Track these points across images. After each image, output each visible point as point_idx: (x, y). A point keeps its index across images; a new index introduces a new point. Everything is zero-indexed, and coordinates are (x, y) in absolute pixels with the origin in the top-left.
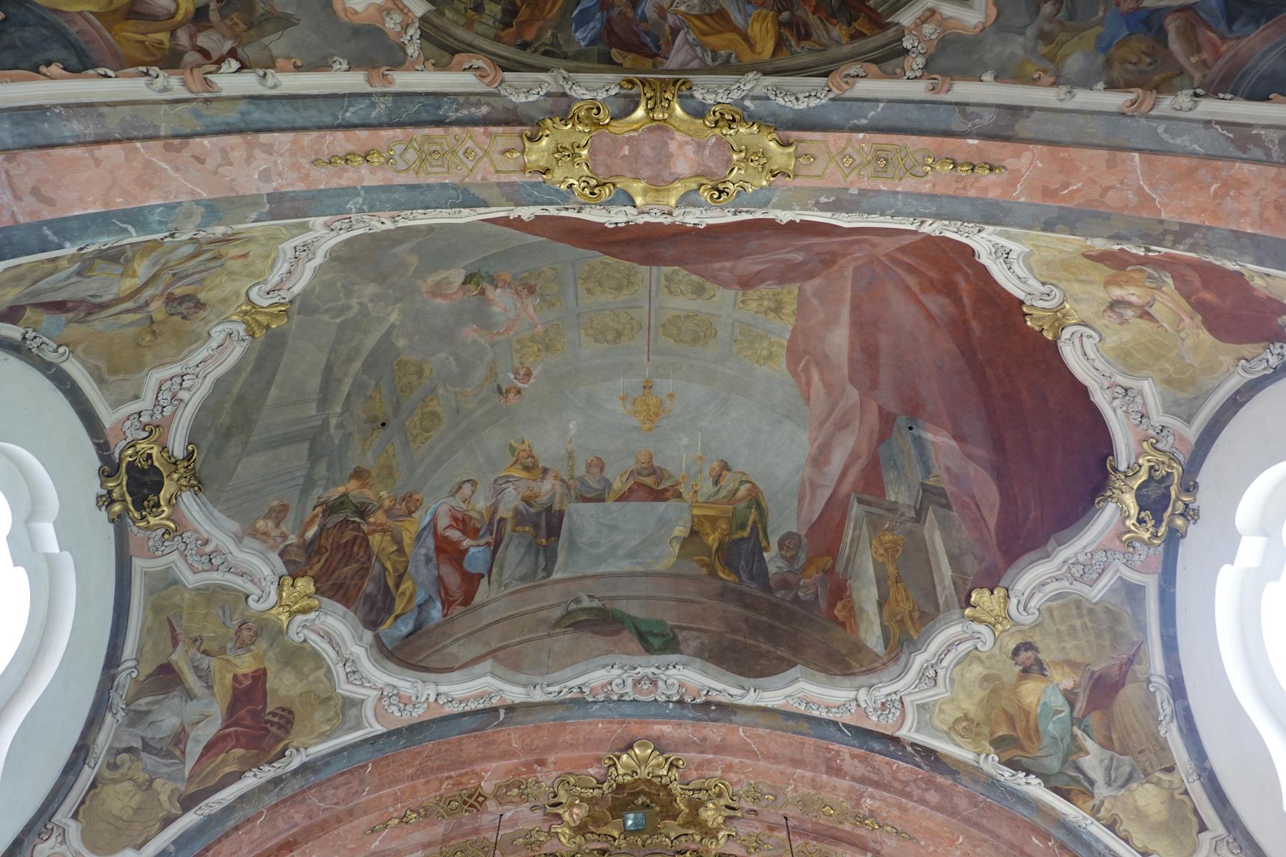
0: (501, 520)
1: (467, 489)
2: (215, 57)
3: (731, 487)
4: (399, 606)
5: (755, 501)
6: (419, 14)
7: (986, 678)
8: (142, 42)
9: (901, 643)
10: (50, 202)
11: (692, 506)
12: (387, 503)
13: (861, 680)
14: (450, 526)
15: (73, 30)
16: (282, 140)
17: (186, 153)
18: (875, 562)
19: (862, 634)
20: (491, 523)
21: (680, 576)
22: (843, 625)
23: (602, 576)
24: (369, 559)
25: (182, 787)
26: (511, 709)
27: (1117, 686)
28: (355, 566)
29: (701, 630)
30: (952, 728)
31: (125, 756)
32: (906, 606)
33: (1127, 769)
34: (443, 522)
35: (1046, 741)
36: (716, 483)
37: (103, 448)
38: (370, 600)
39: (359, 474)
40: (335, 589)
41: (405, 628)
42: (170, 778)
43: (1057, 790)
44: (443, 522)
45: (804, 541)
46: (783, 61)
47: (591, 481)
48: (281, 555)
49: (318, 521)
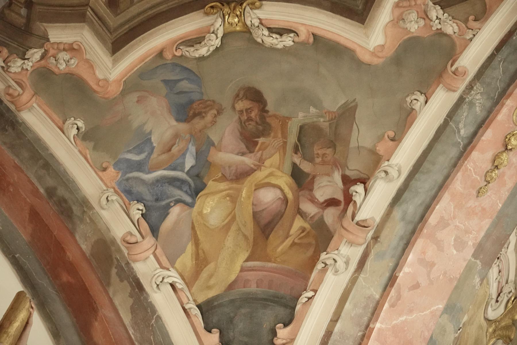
2: (340, 197)
8: (294, 244)
15: (253, 288)
16: (444, 206)
17: (406, 294)
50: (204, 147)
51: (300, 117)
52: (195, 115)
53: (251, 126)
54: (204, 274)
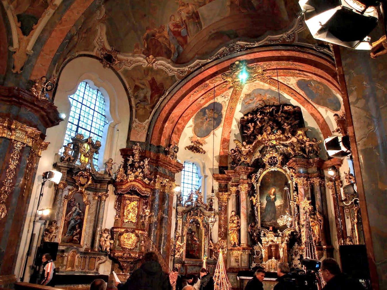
0: (185, 21)
1: (173, 18)
4: (173, 51)
10: (53, 51)
12: (157, 31)
14: (174, 28)
20: (182, 22)
23: (214, 23)
24: (161, 44)
25: (150, 105)
28: (159, 48)
31: (138, 104)
34: (172, 28)
37: (97, 58)
38: (166, 53)
39: (148, 28)
40: (157, 55)
41: (176, 55)
42: (148, 105)
44: (172, 28)
48: (143, 53)
49: (146, 42)
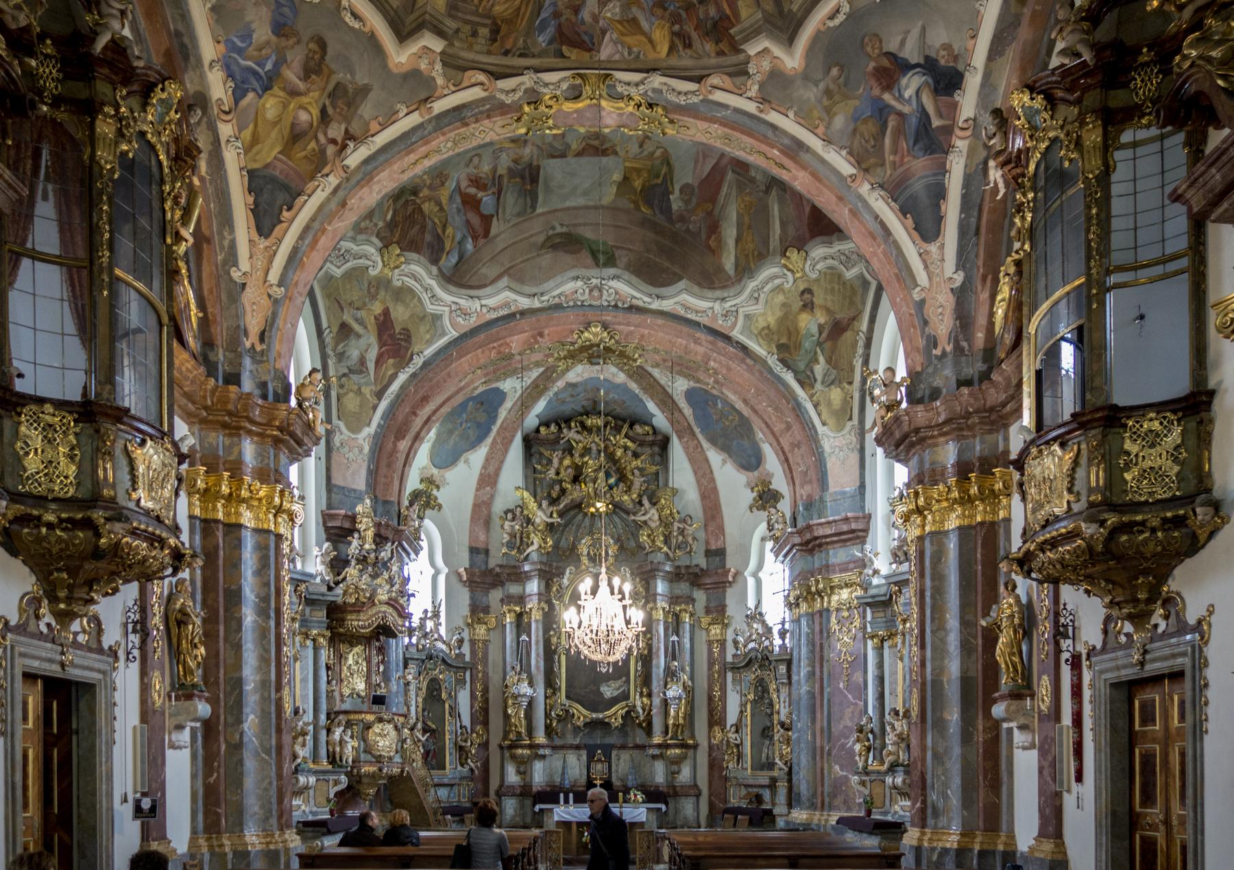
3: (651, 149)
5: (666, 160)
6: (439, 50)
7: (784, 305)
9: (744, 270)
11: (624, 161)
13: (718, 293)
18: (738, 212)
19: (724, 260)
21: (617, 209)
22: (713, 251)
26: (523, 313)
27: (844, 330)
29: (629, 250)
30: (760, 333)
32: (751, 246)
33: (833, 377)
35: (802, 352)
36: (641, 146)
43: (799, 381)
45: (696, 190)
46: (674, 61)
47: (556, 145)
50: (281, 61)
51: (339, 76)
52: (284, 35)
53: (312, 64)
54: (255, 150)
